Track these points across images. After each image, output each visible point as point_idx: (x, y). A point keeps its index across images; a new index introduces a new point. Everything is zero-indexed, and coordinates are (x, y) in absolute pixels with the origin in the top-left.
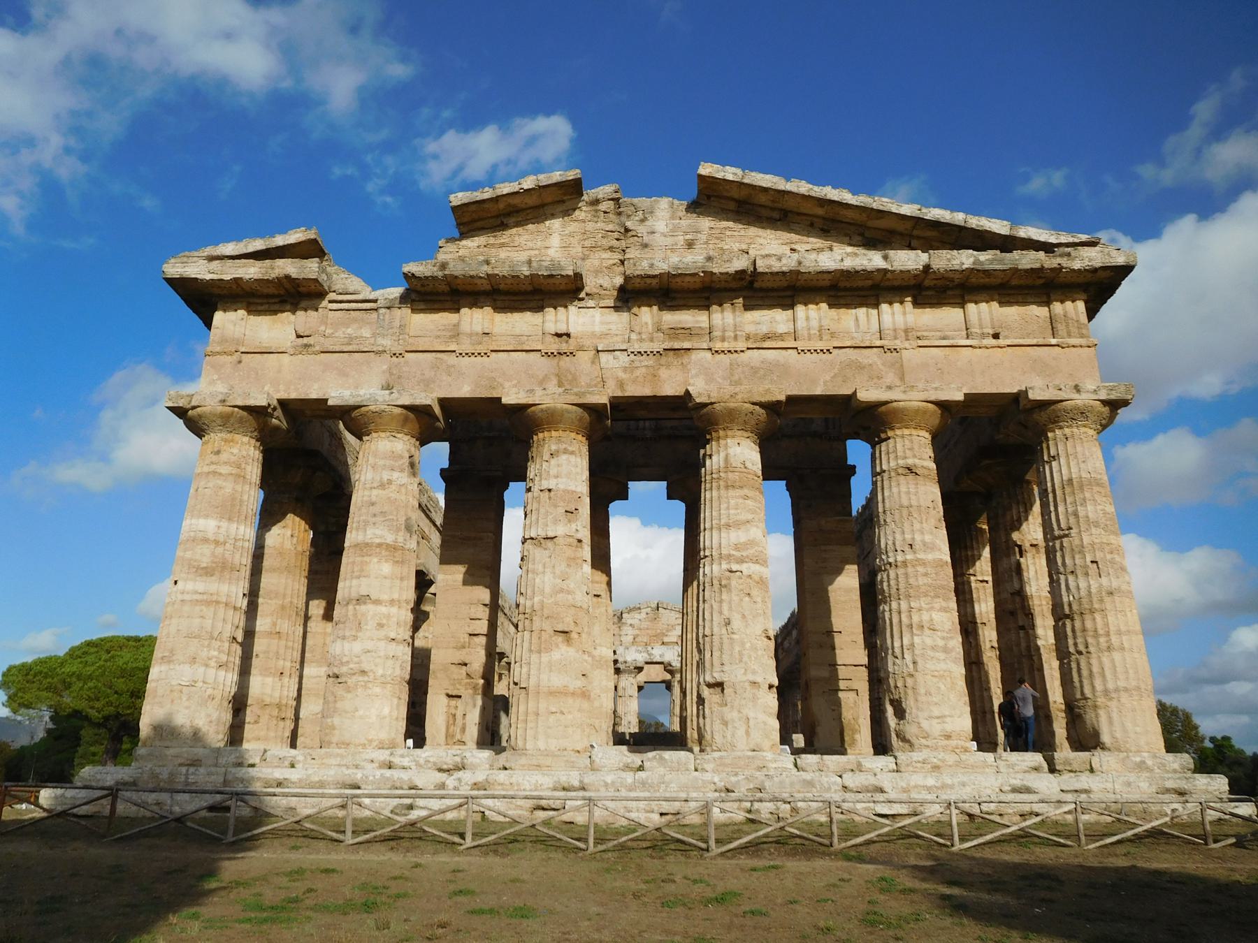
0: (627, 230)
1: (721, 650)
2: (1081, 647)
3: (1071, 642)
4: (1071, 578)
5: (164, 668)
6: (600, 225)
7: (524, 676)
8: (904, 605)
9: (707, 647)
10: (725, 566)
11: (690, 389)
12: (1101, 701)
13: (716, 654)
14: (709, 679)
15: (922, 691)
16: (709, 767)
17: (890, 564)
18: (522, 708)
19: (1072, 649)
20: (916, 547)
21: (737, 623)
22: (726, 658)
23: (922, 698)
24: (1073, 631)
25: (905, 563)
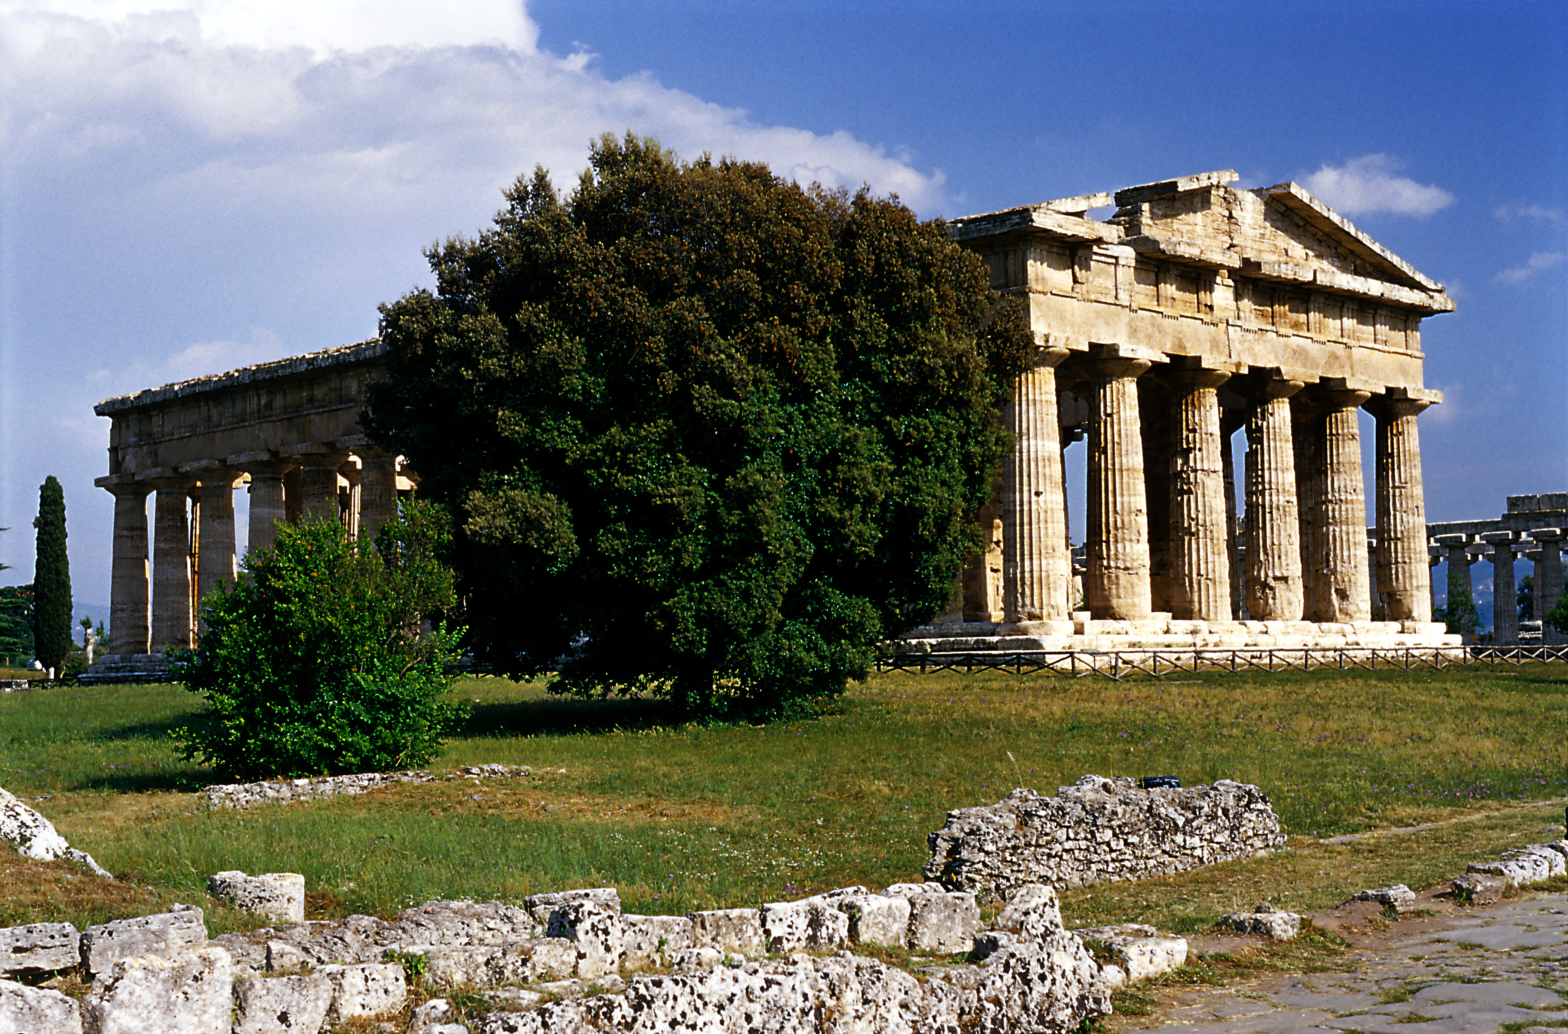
0: (1231, 217)
1: (1286, 555)
2: (1407, 560)
3: (1400, 555)
4: (1404, 515)
5: (1051, 561)
6: (1220, 210)
7: (1210, 571)
8: (1351, 529)
9: (1276, 552)
10: (1287, 498)
11: (1282, 368)
12: (1415, 592)
13: (1283, 557)
14: (1278, 574)
15: (1359, 584)
16: (1291, 630)
17: (1341, 501)
18: (1211, 592)
19: (1400, 560)
20: (1358, 490)
21: (1293, 538)
22: (1289, 562)
23: (1359, 589)
24: (1403, 548)
25: (1352, 501)
